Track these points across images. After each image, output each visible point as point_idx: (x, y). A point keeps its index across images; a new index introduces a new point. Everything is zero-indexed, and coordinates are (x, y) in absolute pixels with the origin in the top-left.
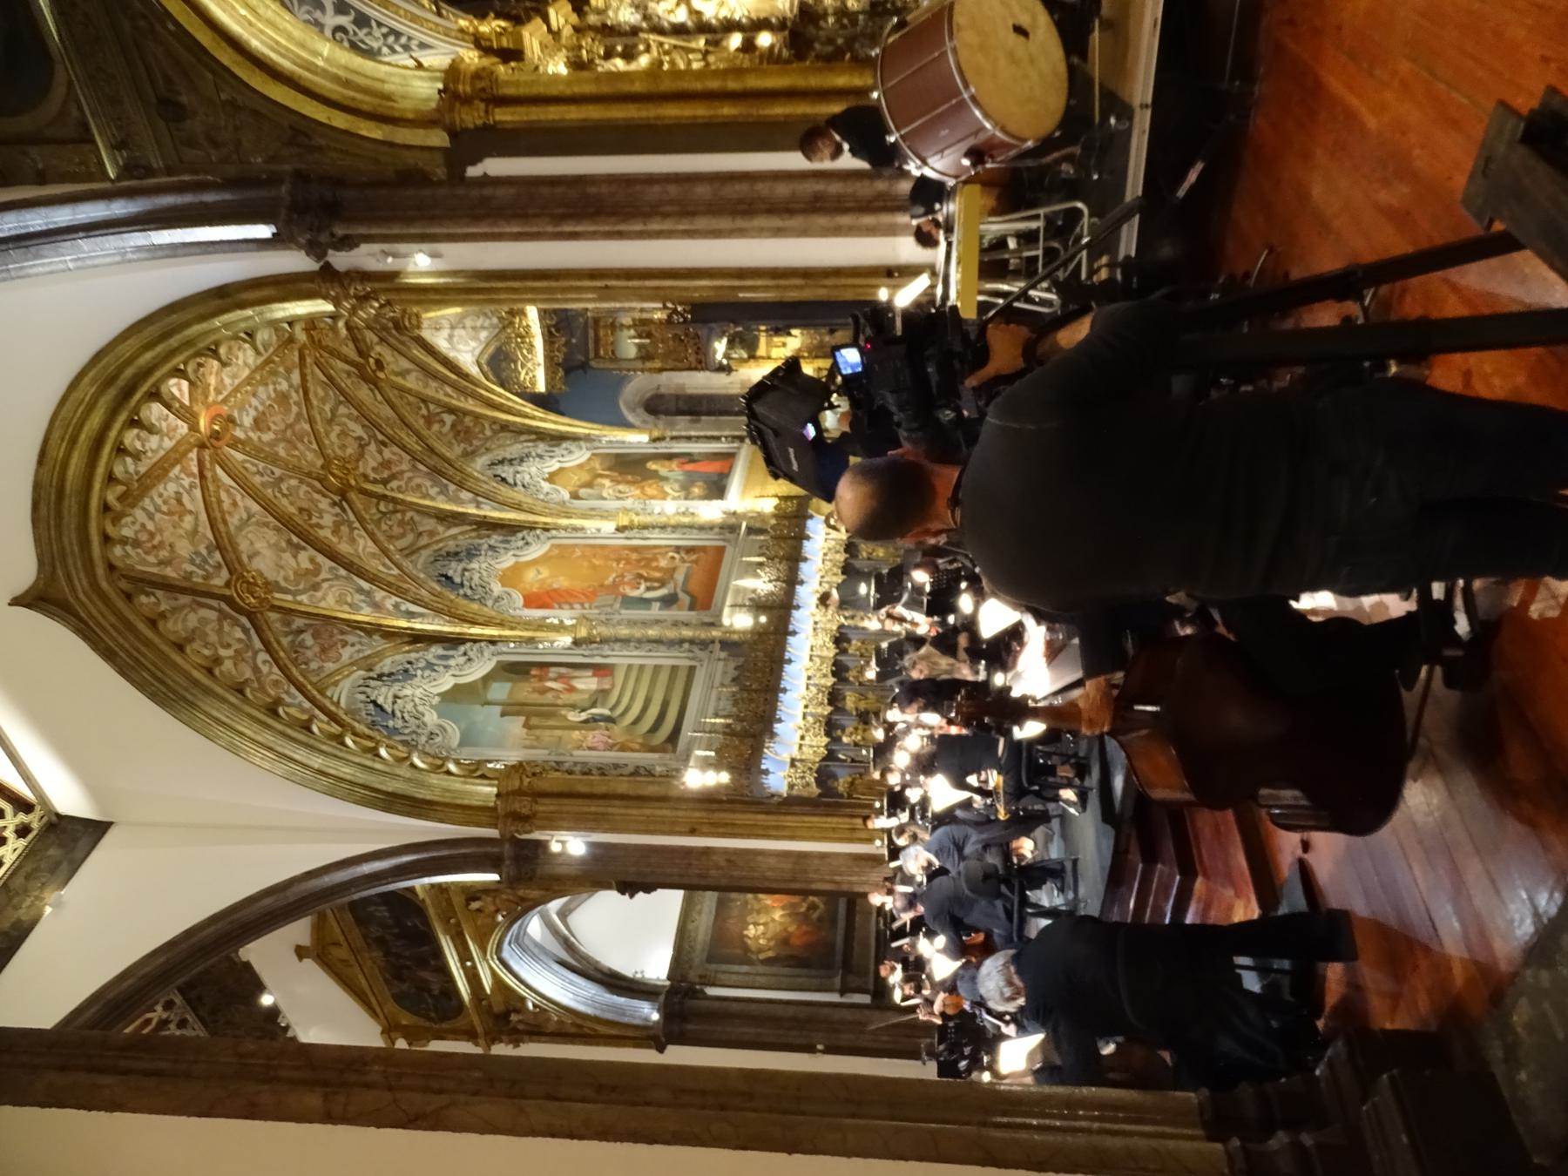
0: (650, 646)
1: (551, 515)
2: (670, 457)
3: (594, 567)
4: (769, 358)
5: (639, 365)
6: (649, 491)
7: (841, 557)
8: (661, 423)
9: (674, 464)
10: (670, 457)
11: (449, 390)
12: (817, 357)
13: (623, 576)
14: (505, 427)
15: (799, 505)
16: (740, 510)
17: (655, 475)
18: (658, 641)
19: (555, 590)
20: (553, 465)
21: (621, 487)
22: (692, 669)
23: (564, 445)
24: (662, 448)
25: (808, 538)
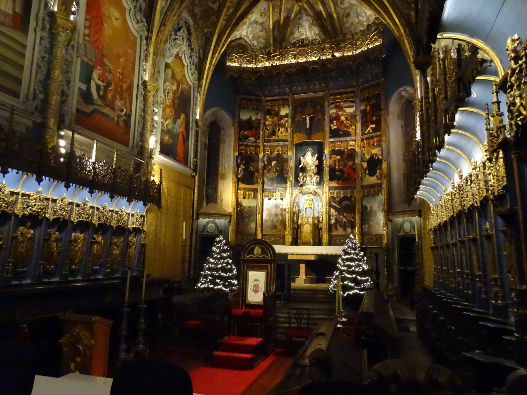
0: (44, 70)
1: (156, 43)
2: (187, 128)
3: (119, 57)
4: (238, 189)
5: (237, 120)
6: (168, 110)
7: (114, 223)
8: (204, 128)
9: (182, 129)
10: (187, 128)
11: (231, 10)
12: (237, 215)
13: (110, 72)
14: (208, 41)
15: (154, 197)
16: (153, 161)
17: (177, 117)
18: (49, 75)
19: (102, 23)
20: (186, 62)
21: (171, 94)
22: (16, 95)
23: (196, 72)
24: (192, 125)
25: (129, 201)
